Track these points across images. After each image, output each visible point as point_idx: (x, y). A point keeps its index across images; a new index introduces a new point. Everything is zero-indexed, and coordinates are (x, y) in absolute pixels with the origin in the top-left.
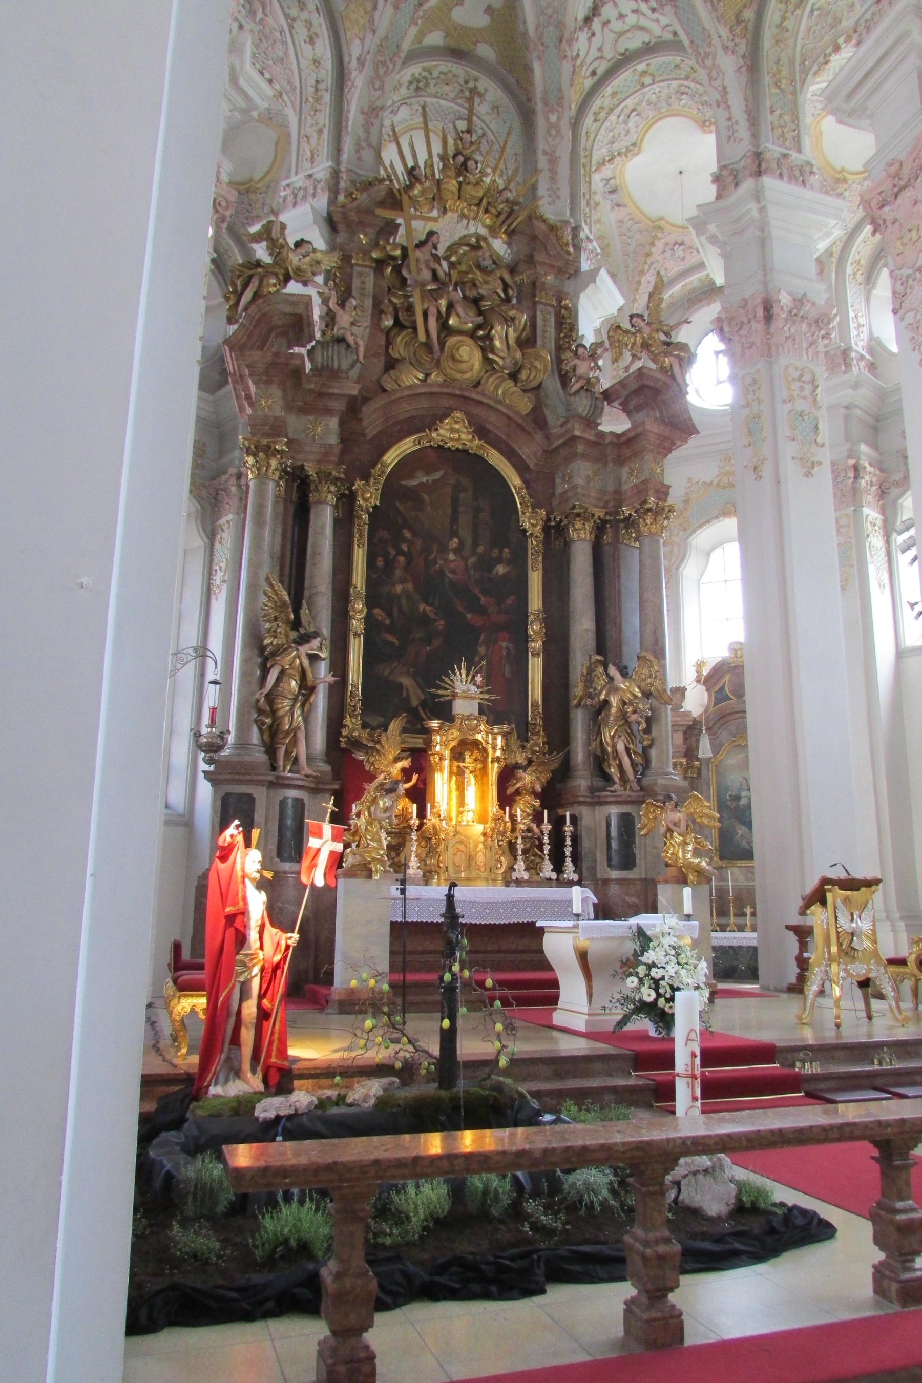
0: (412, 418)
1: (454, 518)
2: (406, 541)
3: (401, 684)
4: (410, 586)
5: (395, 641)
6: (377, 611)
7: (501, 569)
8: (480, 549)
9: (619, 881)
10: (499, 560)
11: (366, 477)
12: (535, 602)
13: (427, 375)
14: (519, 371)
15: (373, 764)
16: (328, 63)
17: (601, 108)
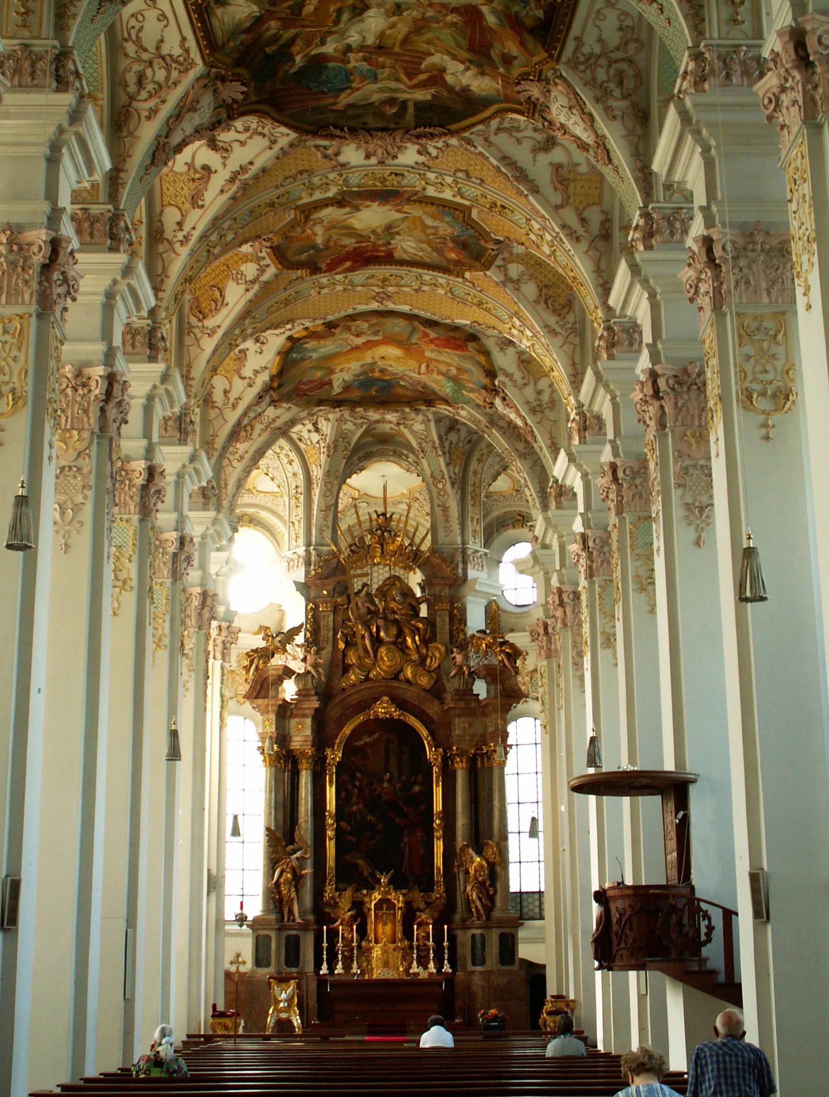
0: (360, 702)
1: (387, 762)
2: (357, 779)
3: (357, 865)
4: (361, 806)
5: (354, 840)
6: (343, 824)
7: (417, 788)
8: (404, 778)
9: (481, 972)
10: (415, 783)
11: (332, 746)
12: (438, 804)
13: (369, 672)
14: (425, 659)
15: (335, 914)
16: (301, 477)
17: (482, 455)
